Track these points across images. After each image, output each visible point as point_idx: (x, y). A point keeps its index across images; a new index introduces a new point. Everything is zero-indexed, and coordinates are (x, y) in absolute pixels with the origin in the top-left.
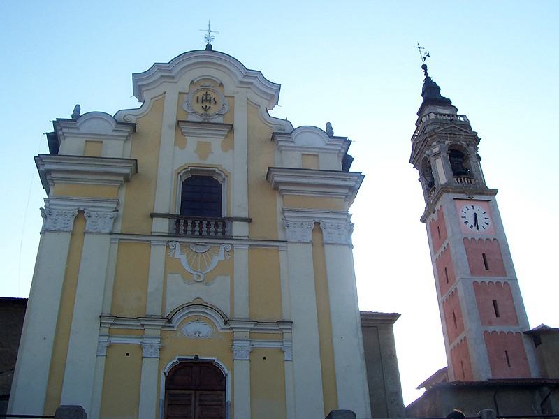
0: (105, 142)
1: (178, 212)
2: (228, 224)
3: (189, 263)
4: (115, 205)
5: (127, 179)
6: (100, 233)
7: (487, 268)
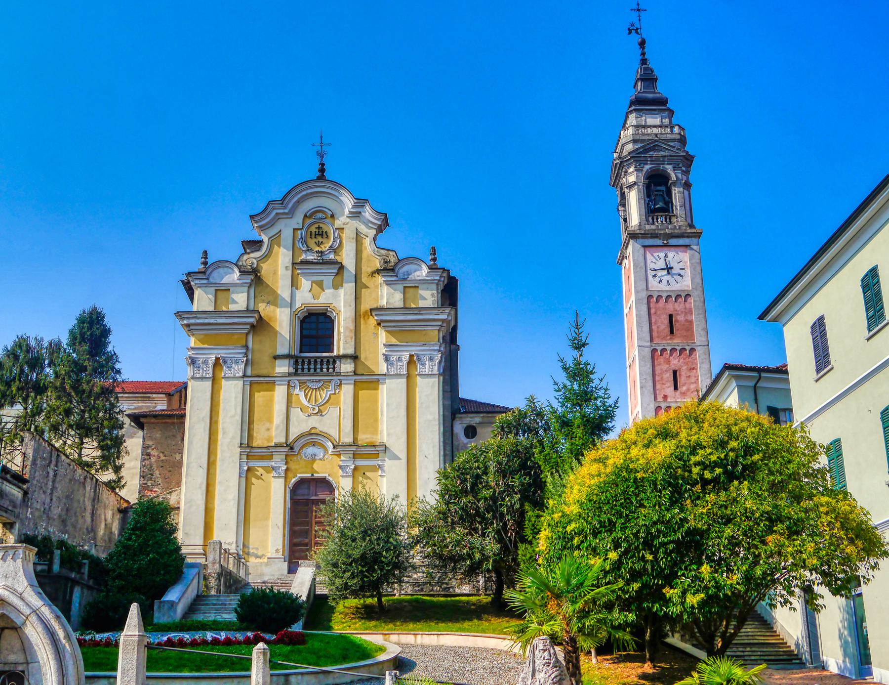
0: (231, 289)
1: (295, 351)
2: (338, 362)
3: (306, 396)
4: (244, 351)
5: (253, 326)
6: (234, 378)
7: (672, 332)
